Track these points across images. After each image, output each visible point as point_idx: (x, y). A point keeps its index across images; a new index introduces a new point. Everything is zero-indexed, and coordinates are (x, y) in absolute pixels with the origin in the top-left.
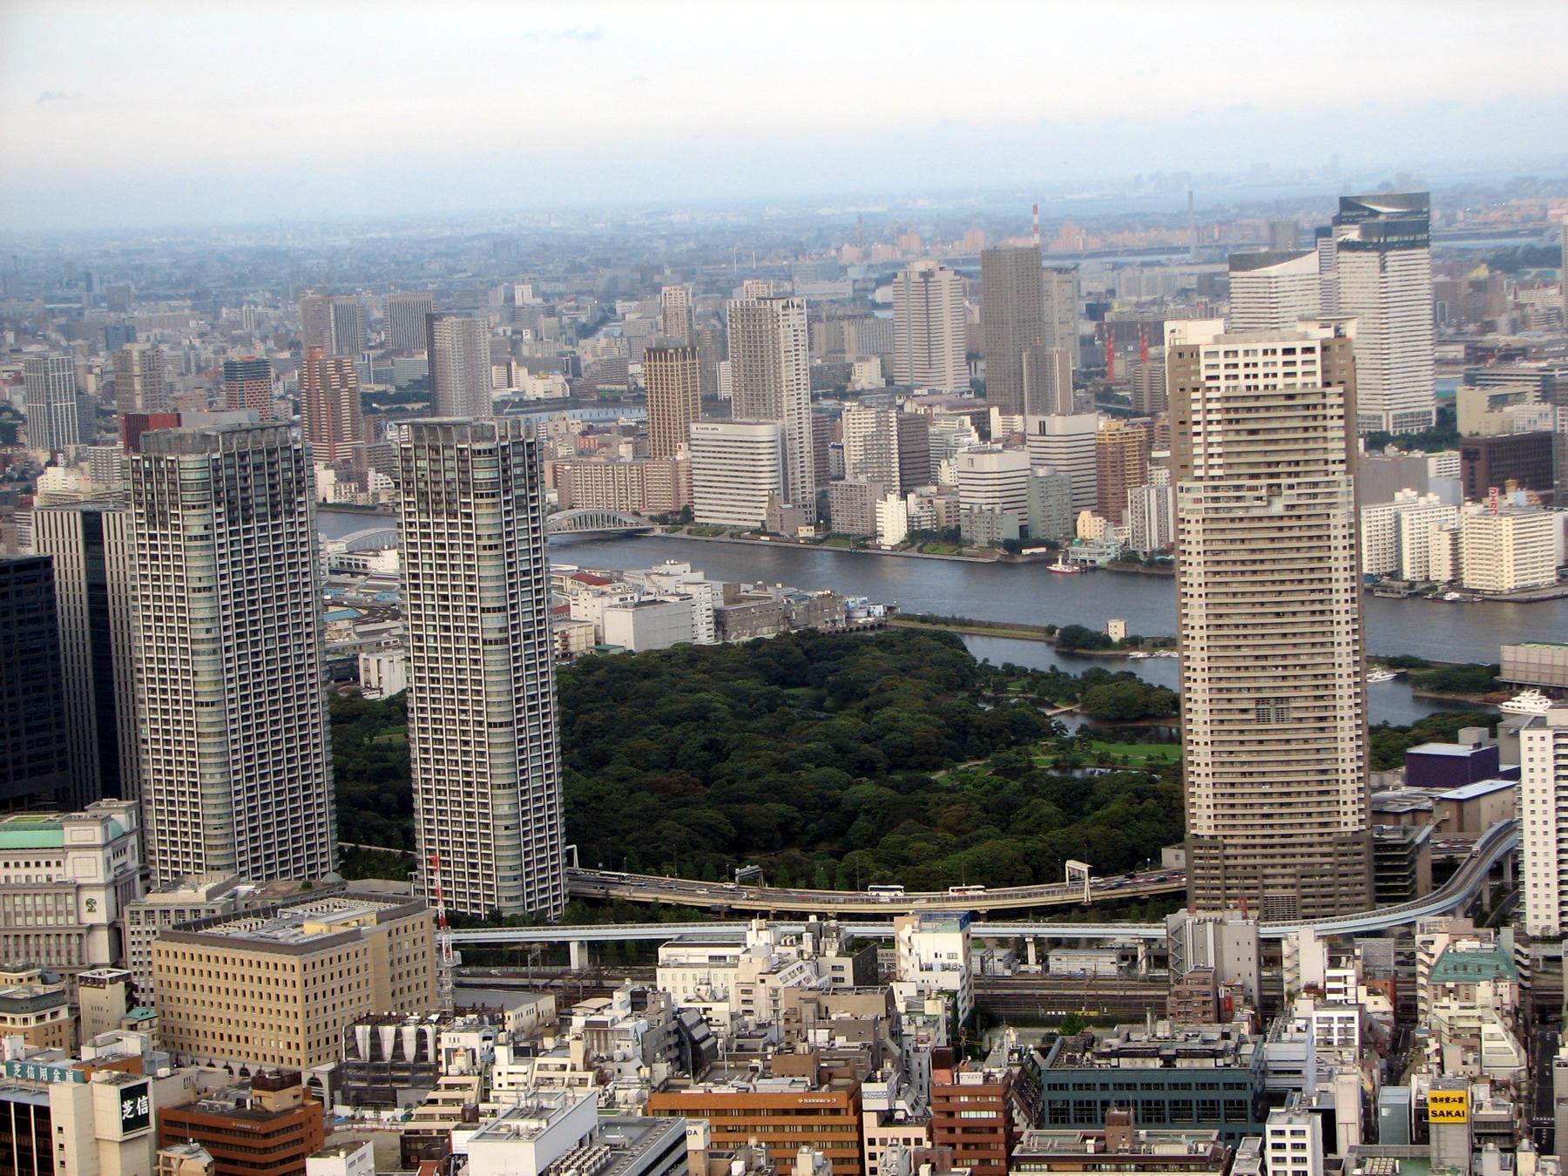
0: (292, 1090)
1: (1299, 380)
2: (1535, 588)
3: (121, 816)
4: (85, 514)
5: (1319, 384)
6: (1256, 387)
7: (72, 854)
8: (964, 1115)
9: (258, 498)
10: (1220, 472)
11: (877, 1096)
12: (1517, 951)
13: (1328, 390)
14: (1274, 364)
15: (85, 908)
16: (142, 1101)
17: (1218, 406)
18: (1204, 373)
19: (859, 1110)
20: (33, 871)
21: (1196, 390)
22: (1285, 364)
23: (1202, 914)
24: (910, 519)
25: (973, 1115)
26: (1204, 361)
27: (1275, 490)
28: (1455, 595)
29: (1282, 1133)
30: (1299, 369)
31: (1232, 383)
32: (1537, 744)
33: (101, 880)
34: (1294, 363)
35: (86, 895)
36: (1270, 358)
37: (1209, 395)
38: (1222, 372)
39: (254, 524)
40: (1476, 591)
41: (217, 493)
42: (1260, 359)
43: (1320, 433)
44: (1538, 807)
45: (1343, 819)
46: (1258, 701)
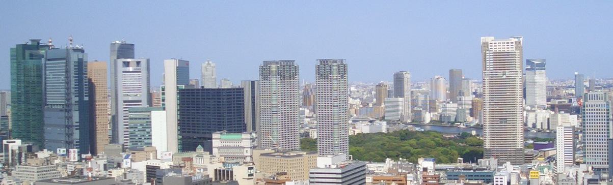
0: (285, 176)
1: (510, 49)
7: (243, 140)
8: (429, 182)
9: (287, 75)
11: (411, 177)
15: (245, 152)
16: (252, 170)
18: (489, 47)
19: (406, 181)
23: (485, 160)
24: (431, 118)
25: (431, 182)
26: (489, 45)
28: (548, 131)
29: (497, 178)
30: (510, 47)
31: (495, 50)
32: (560, 130)
33: (249, 146)
36: (504, 44)
38: (493, 47)
39: (286, 81)
40: (552, 130)
41: (278, 73)
43: (514, 61)
44: (560, 143)
46: (500, 119)
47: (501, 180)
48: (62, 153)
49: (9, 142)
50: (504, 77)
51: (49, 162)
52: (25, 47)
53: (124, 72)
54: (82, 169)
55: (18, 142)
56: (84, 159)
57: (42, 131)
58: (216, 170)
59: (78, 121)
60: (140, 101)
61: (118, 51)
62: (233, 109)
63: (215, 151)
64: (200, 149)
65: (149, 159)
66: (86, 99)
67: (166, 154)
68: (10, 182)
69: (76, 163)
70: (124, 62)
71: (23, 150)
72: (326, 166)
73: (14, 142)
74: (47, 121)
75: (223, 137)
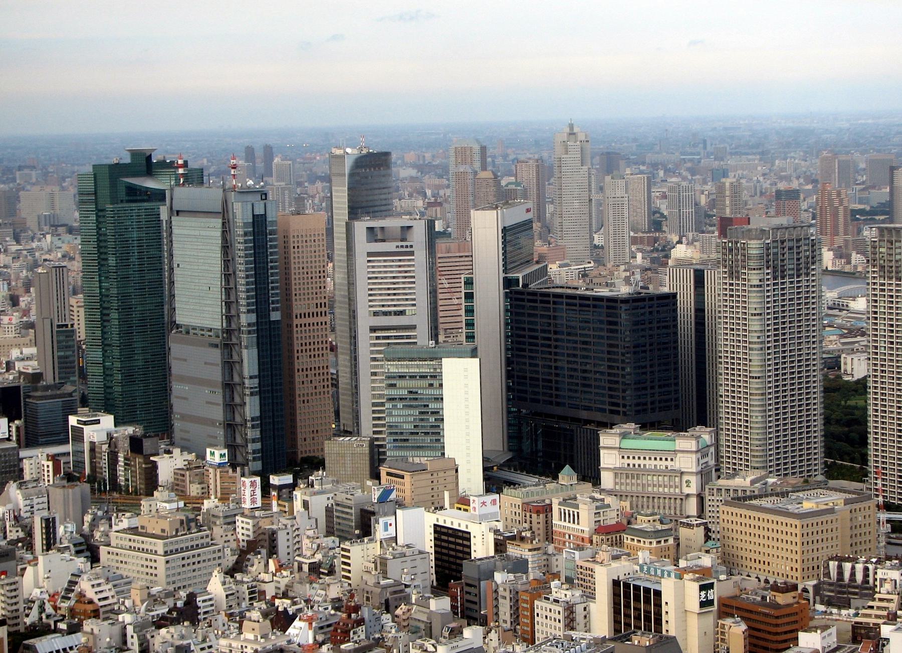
0: (793, 594)
3: (706, 435)
4: (696, 271)
7: (679, 455)
9: (790, 265)
15: (684, 485)
16: (711, 592)
20: (658, 462)
33: (694, 470)
35: (685, 478)
39: (787, 280)
41: (768, 262)
48: (217, 460)
49: (85, 423)
51: (193, 524)
52: (116, 170)
53: (370, 254)
54: (274, 533)
55: (107, 421)
56: (275, 487)
57: (164, 391)
58: (616, 583)
59: (256, 373)
60: (413, 327)
61: (351, 175)
62: (649, 369)
63: (607, 480)
64: (567, 476)
65: (442, 508)
66: (275, 316)
67: (484, 503)
68: (99, 585)
69: (257, 513)
70: (370, 230)
71: (120, 444)
73: (98, 422)
74: (176, 368)
75: (628, 443)
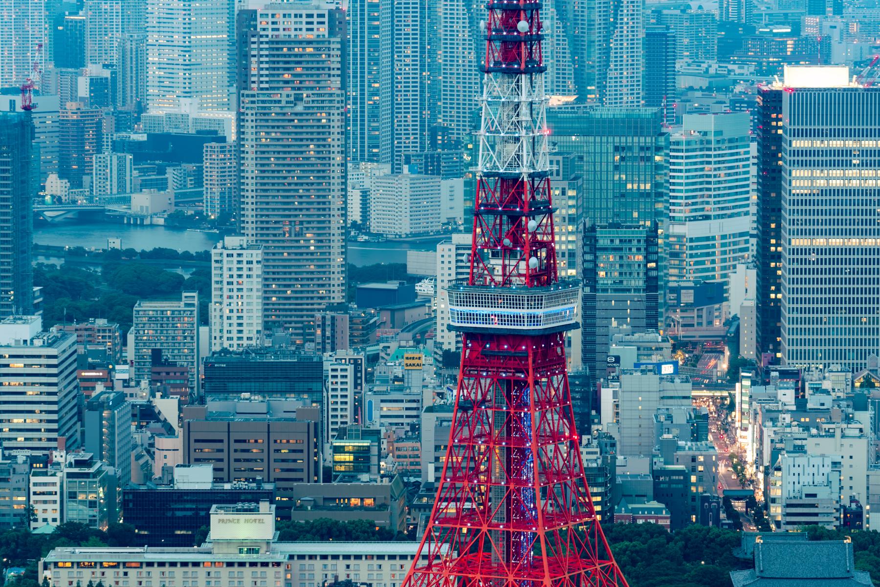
2: (427, 233)
5: (327, 36)
6: (289, 36)
10: (267, 86)
11: (123, 371)
12: (436, 353)
13: (332, 40)
14: (301, 23)
17: (267, 46)
21: (253, 36)
22: (307, 23)
27: (298, 98)
31: (276, 33)
34: (312, 23)
36: (298, 19)
37: (261, 39)
42: (293, 19)
45: (332, 295)
47: (344, 374)
50: (299, 108)
72: (17, 341)
